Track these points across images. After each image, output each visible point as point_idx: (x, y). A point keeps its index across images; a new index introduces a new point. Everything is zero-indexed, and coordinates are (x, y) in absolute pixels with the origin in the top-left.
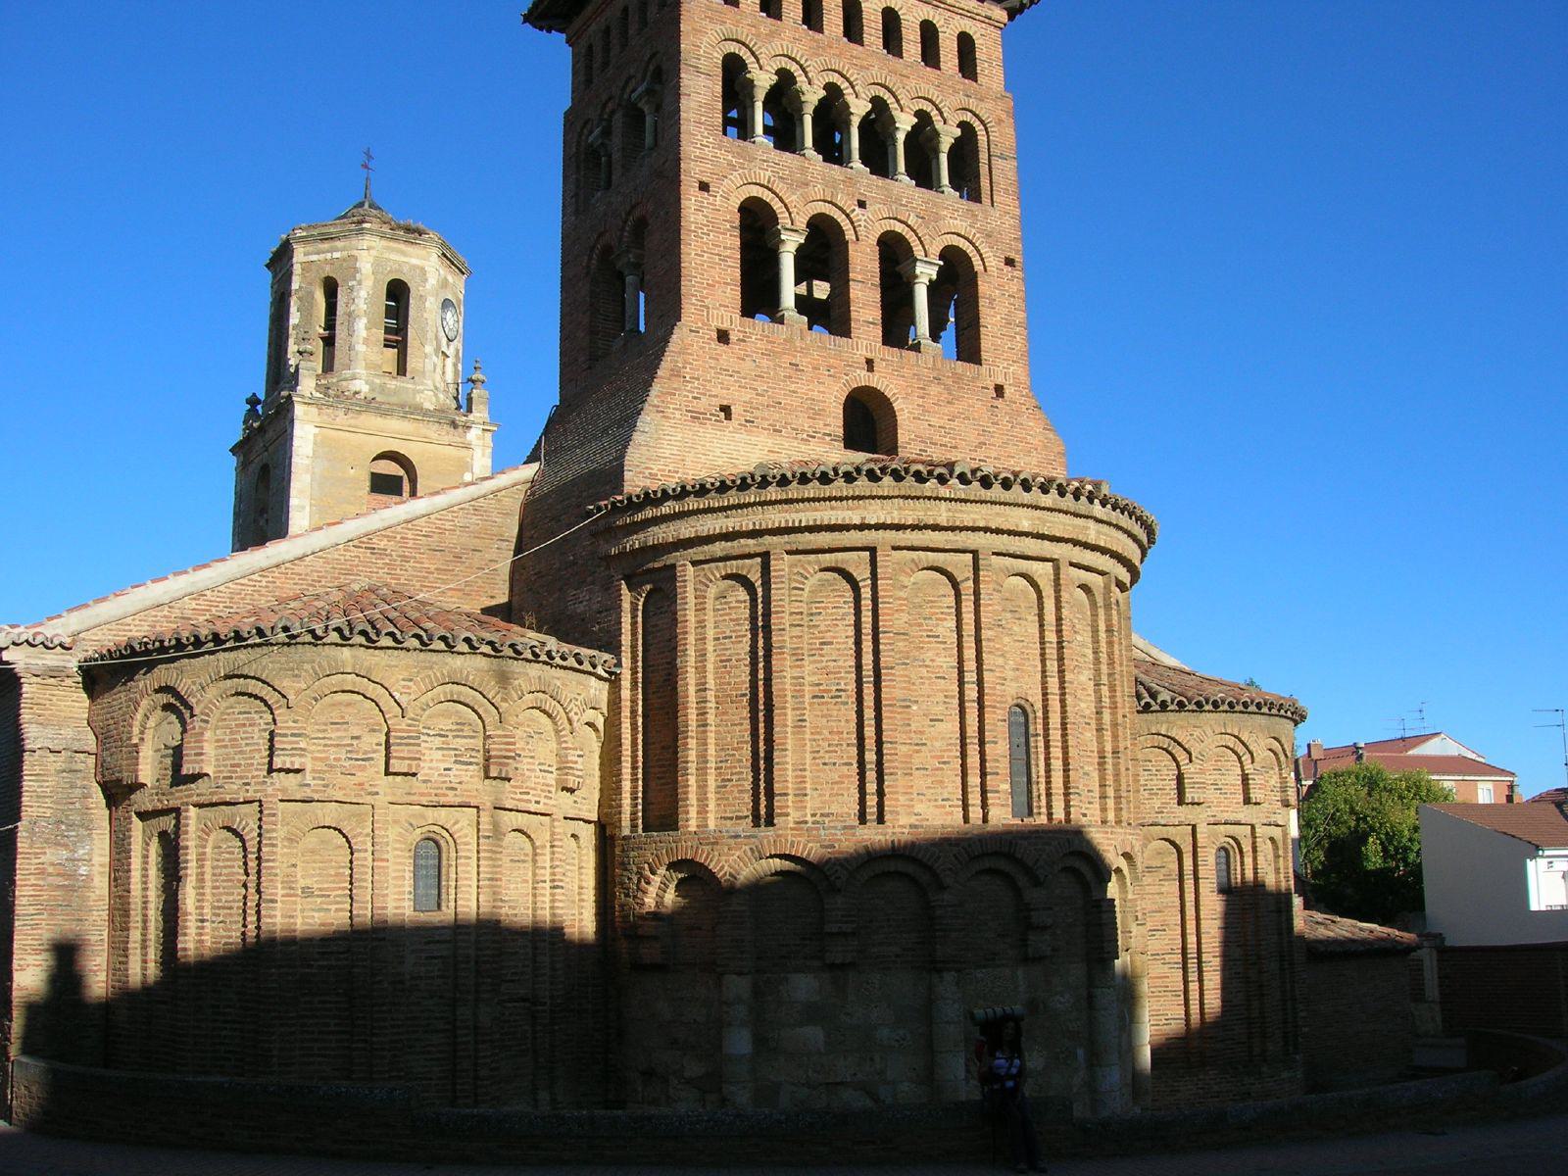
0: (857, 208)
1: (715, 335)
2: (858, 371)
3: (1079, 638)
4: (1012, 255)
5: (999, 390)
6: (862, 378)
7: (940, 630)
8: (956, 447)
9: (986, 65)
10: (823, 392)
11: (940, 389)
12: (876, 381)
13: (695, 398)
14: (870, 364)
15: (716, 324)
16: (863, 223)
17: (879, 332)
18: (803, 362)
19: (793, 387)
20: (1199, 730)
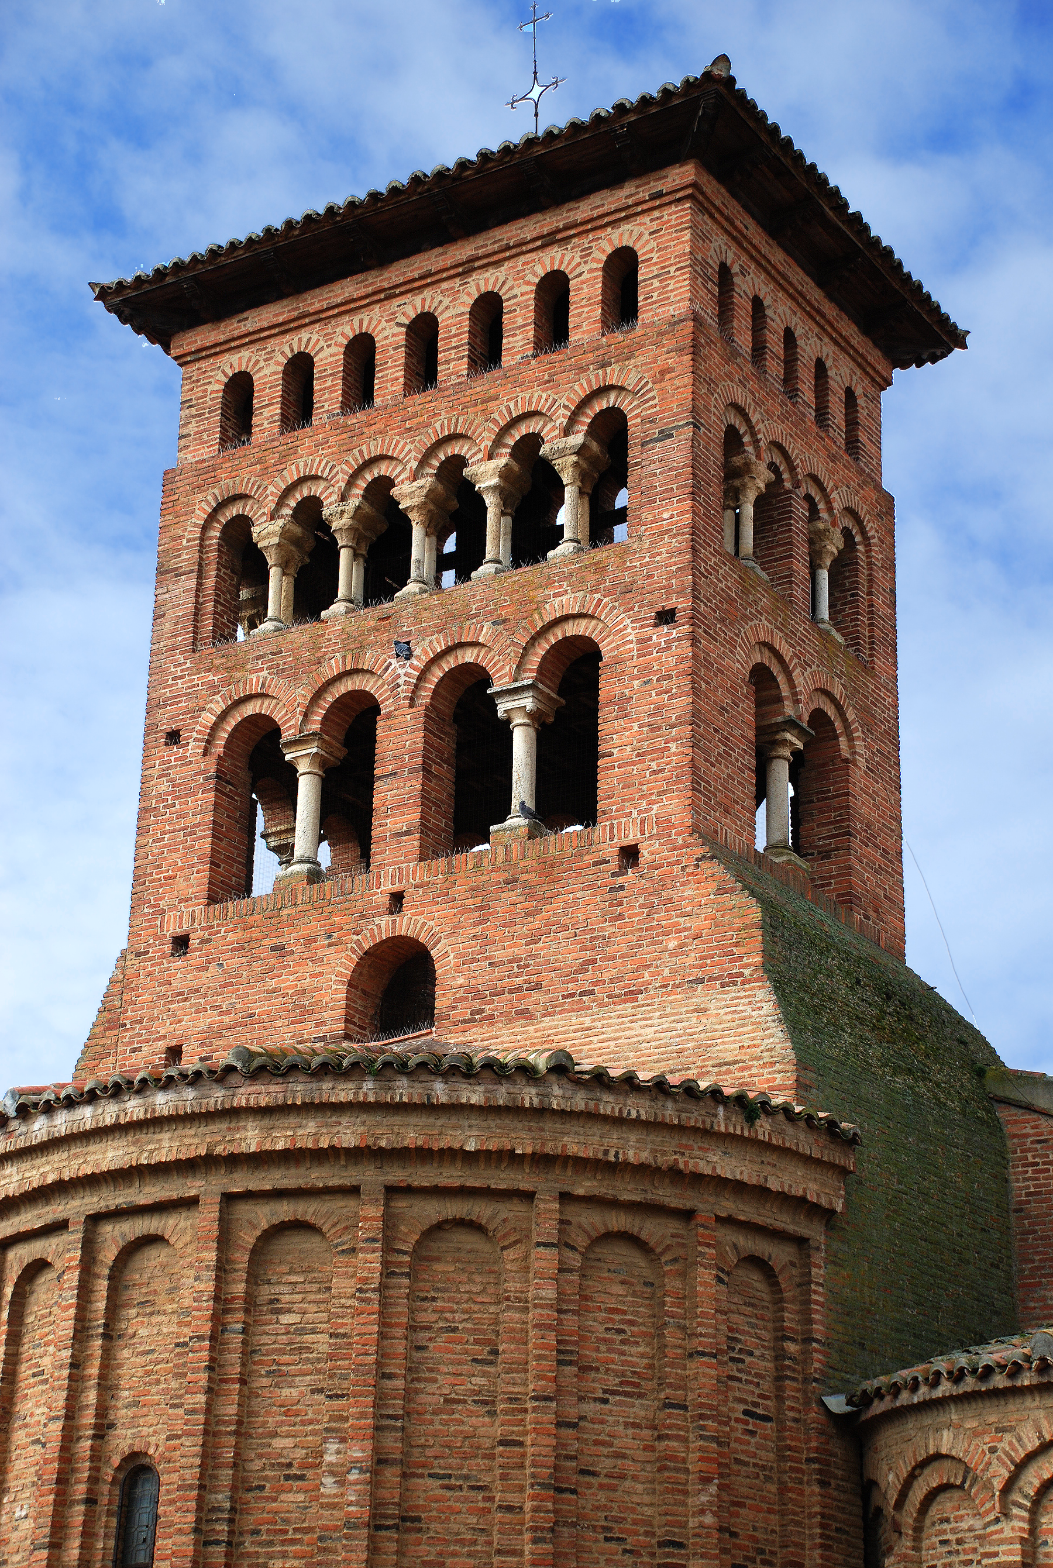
0: (394, 661)
1: (168, 948)
2: (377, 920)
3: (286, 1319)
4: (668, 605)
5: (630, 855)
6: (384, 927)
7: (46, 1361)
8: (537, 987)
9: (656, 283)
10: (321, 974)
11: (512, 895)
12: (406, 924)
13: (134, 1050)
14: (397, 899)
15: (172, 929)
16: (401, 681)
17: (413, 843)
18: (290, 938)
19: (272, 984)
20: (1008, 1437)
